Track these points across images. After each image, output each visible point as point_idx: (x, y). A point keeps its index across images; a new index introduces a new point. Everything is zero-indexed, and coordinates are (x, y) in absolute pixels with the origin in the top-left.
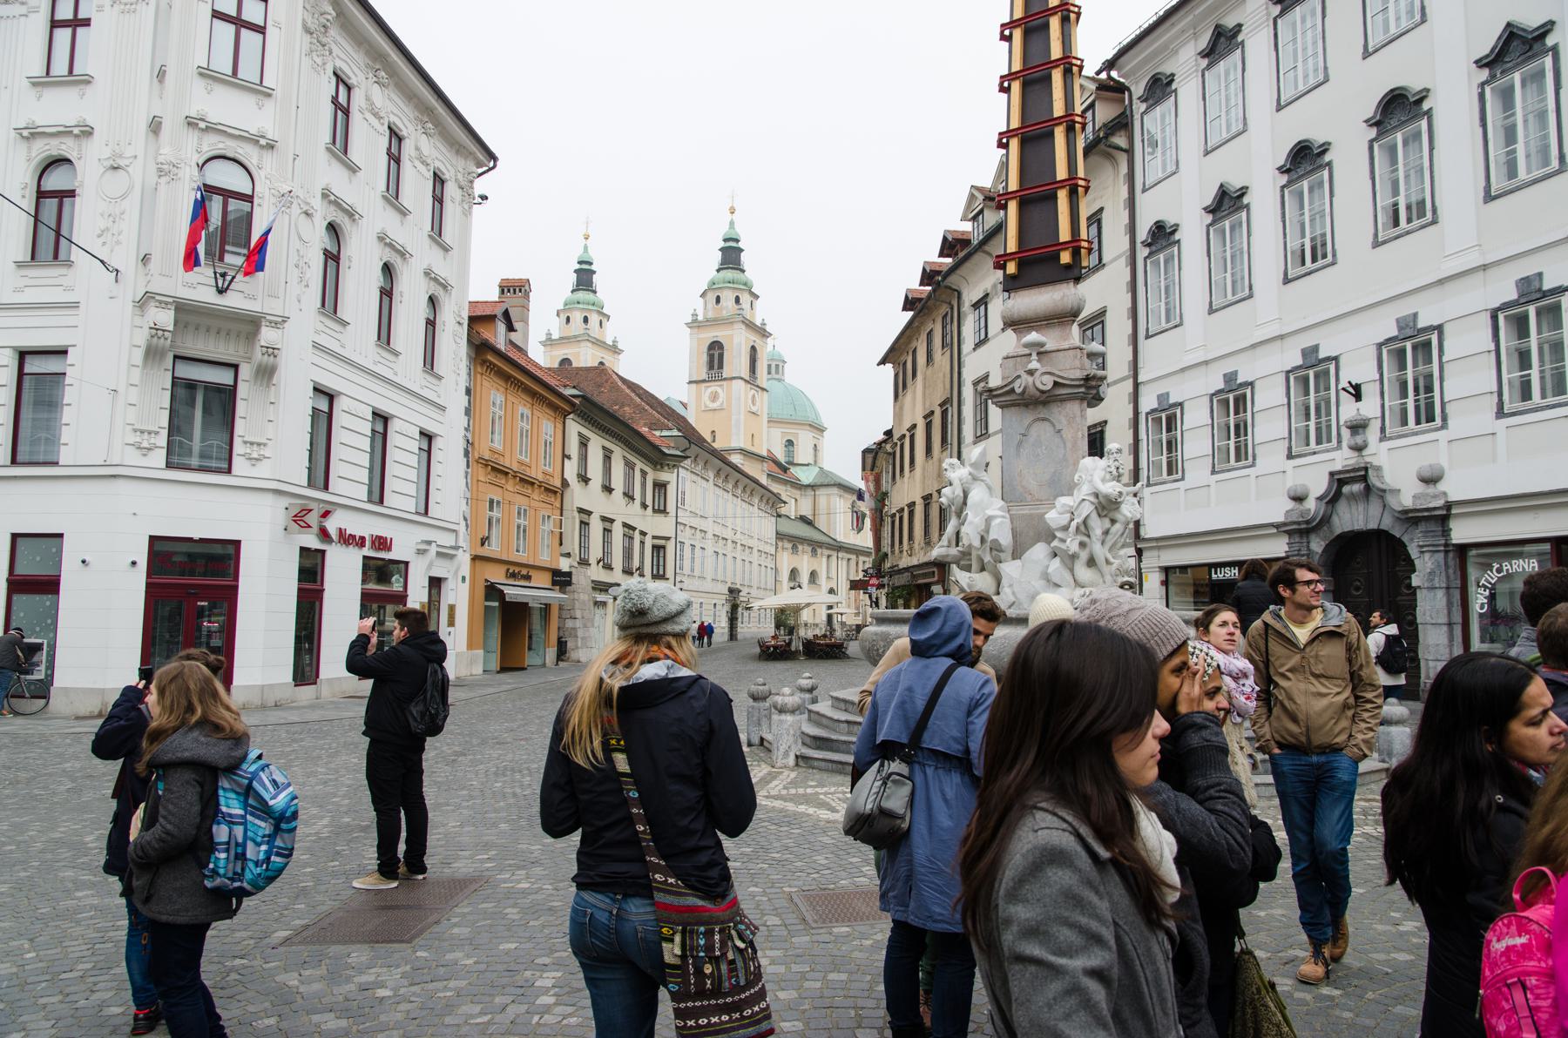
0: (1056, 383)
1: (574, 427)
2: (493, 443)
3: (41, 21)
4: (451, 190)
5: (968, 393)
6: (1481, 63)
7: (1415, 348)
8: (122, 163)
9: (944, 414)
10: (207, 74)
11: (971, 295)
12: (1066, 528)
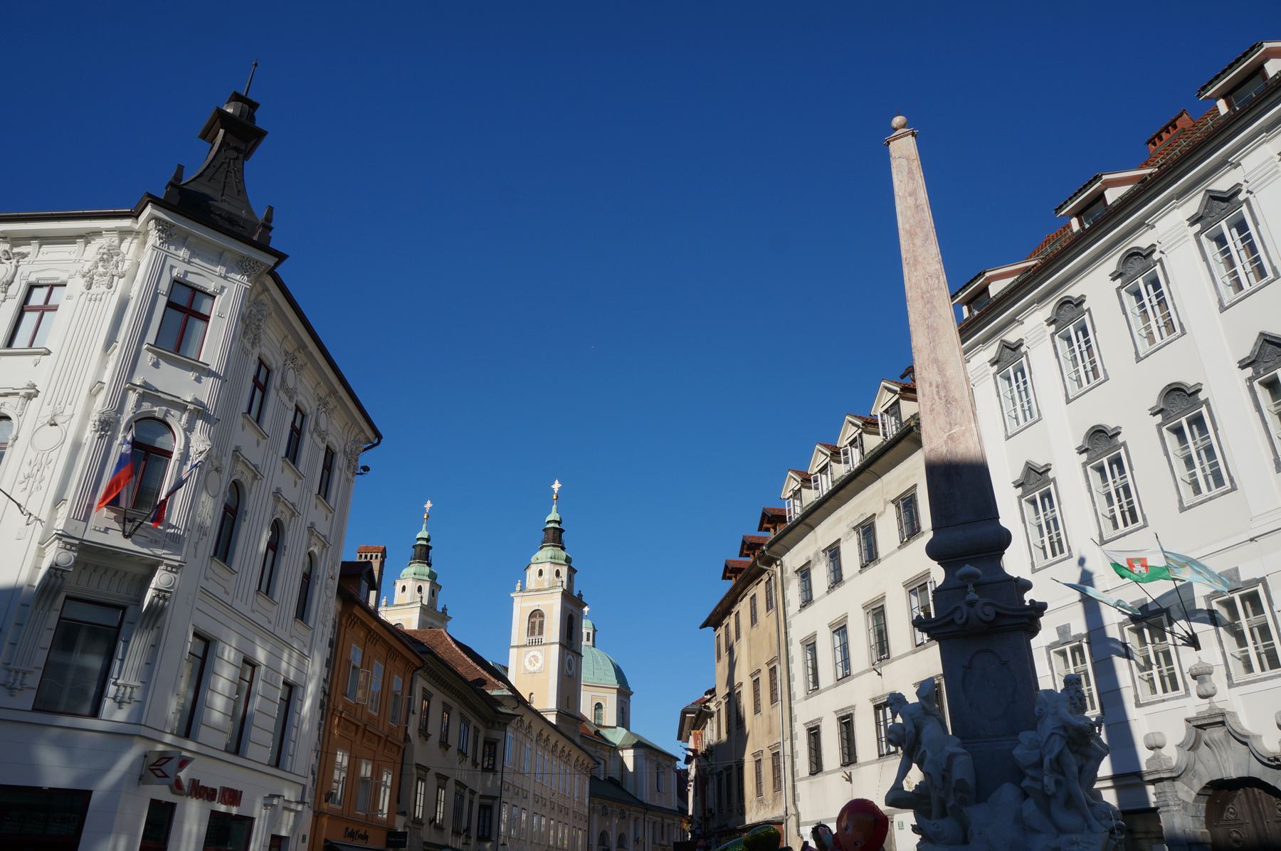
0: (997, 614)
1: (421, 683)
3: (12, 306)
4: (340, 461)
5: (797, 651)
6: (1243, 365)
7: (1243, 598)
8: (58, 420)
9: (773, 671)
12: (1039, 764)
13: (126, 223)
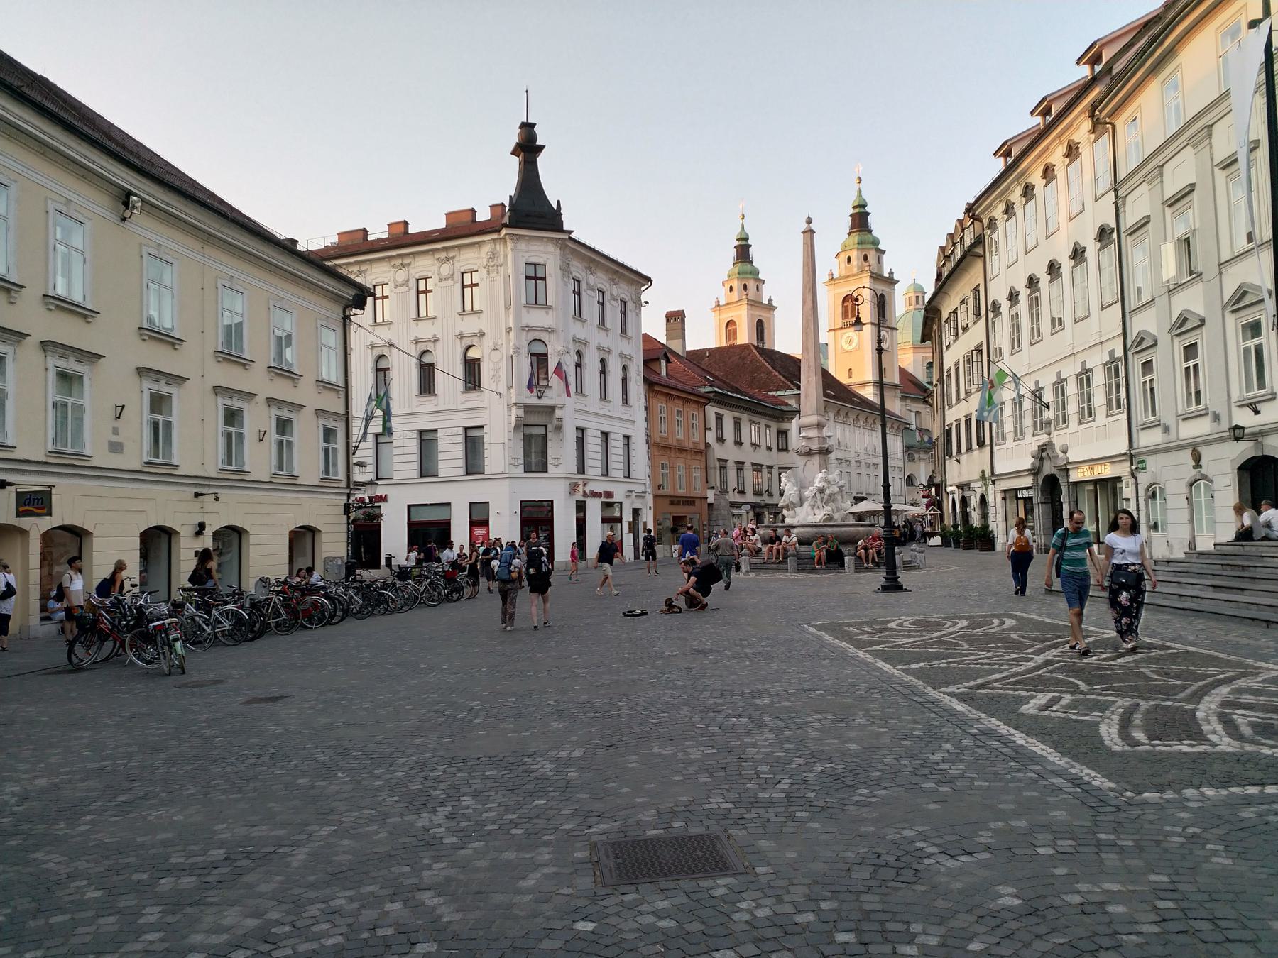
1: (712, 411)
2: (661, 432)
4: (630, 306)
10: (527, 305)
11: (945, 315)
13: (495, 236)
